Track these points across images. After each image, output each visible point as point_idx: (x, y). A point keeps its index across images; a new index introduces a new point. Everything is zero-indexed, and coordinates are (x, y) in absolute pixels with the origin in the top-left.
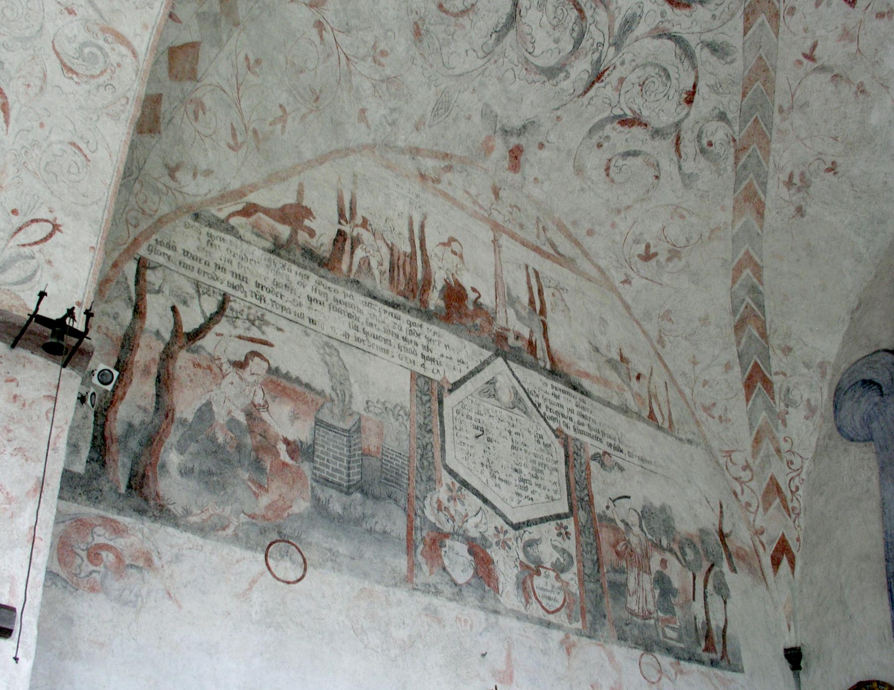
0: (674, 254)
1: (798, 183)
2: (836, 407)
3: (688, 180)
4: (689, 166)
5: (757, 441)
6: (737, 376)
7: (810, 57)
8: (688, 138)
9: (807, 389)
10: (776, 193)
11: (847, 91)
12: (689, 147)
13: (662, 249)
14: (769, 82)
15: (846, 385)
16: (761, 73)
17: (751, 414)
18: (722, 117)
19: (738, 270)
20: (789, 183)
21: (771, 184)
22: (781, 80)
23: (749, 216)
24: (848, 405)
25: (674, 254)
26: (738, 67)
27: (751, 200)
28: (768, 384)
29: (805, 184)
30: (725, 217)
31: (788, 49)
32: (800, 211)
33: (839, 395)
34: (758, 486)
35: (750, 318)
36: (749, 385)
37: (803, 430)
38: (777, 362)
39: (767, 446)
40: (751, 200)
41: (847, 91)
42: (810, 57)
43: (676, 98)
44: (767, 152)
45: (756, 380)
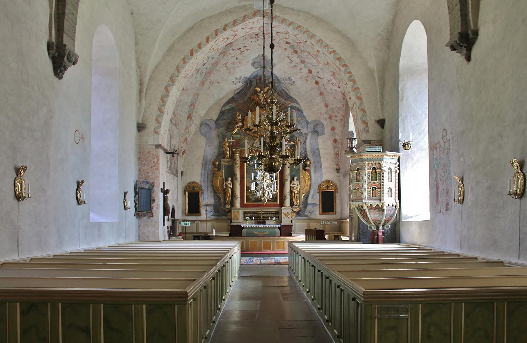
0: (187, 90)
1: (212, 83)
2: (201, 127)
3: (196, 78)
4: (197, 76)
5: (186, 129)
6: (187, 115)
7: (226, 64)
8: (200, 71)
9: (197, 121)
10: (207, 83)
11: (228, 72)
12: (199, 73)
13: (185, 89)
14: (217, 65)
15: (204, 122)
16: (217, 63)
17: (187, 123)
18: (207, 68)
19: (195, 95)
20: (210, 82)
21: (207, 81)
22: (219, 66)
23: (201, 86)
24: (203, 127)
25: (187, 90)
26: (213, 62)
27: (203, 83)
28: (191, 118)
29: (213, 84)
30: (197, 85)
31: (223, 62)
32: (209, 87)
33: (202, 124)
34: (184, 138)
35: (192, 105)
36: (188, 117)
37: (193, 128)
38: (194, 114)
39: (187, 131)
40: (203, 83)
41: (228, 72)
42: (226, 64)
43: (202, 64)
44: (210, 76)
45: (189, 117)
